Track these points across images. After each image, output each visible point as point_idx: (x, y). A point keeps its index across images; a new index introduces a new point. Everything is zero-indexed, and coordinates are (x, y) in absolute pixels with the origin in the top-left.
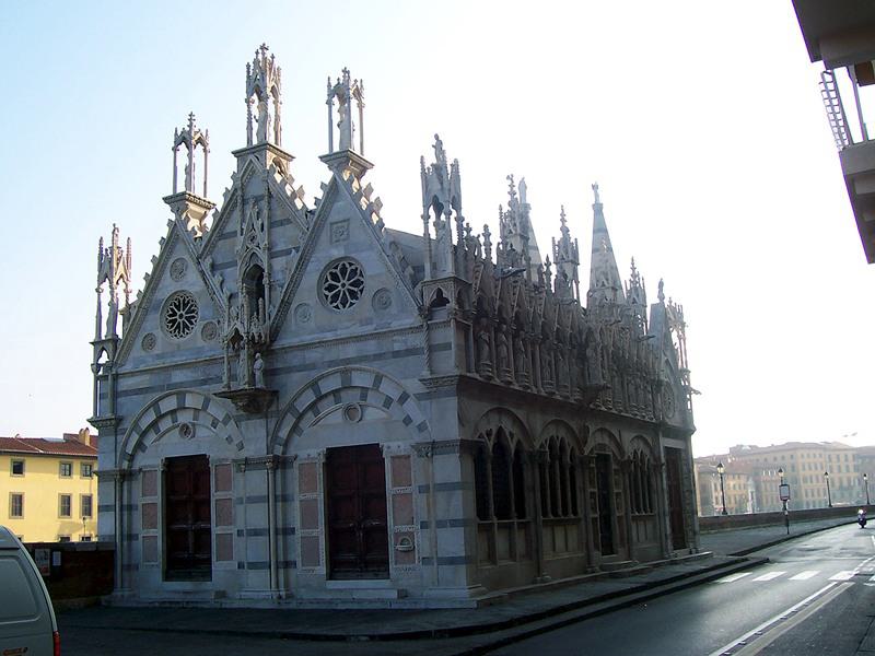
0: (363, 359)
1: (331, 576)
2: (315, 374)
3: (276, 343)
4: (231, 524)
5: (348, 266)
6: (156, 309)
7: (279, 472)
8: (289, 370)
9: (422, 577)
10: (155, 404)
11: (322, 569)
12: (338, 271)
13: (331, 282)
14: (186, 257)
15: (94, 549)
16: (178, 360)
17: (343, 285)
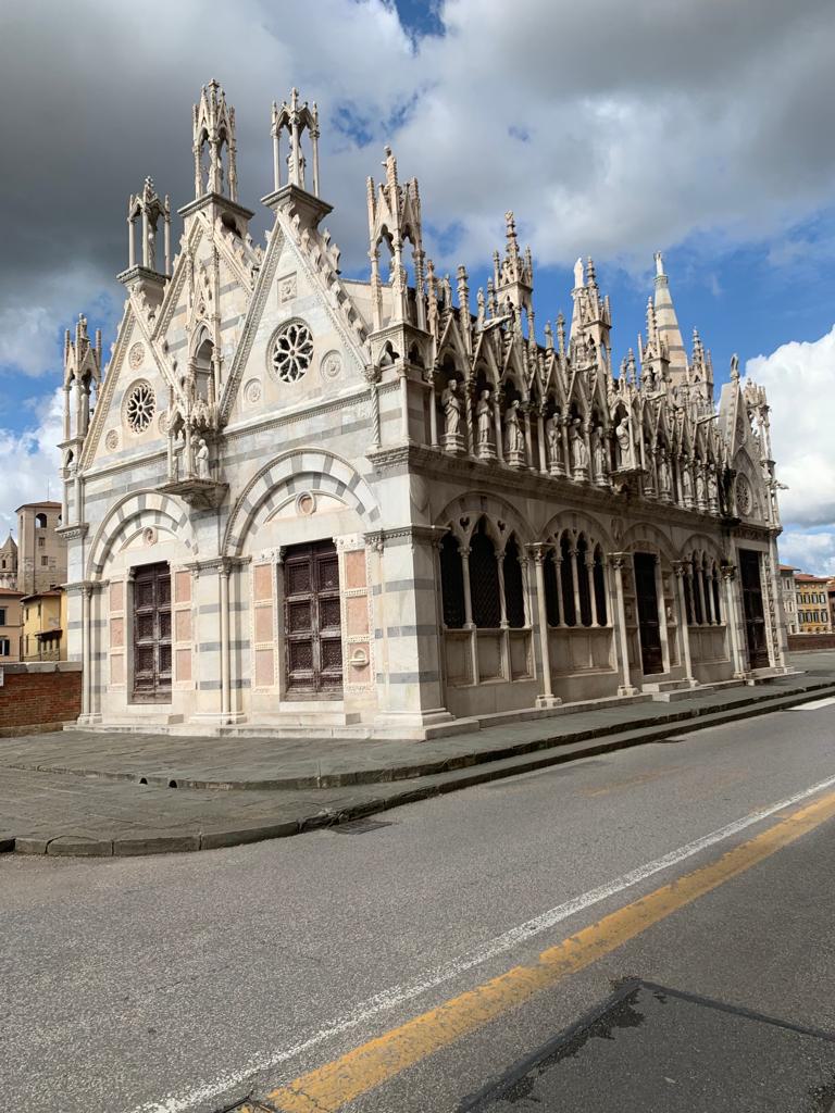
1: (284, 698)
3: (226, 429)
4: (189, 638)
5: (297, 329)
6: (117, 403)
7: (232, 576)
8: (240, 458)
9: (376, 698)
11: (276, 688)
12: (287, 337)
13: (281, 351)
14: (143, 341)
15: (53, 670)
16: (137, 457)
17: (293, 353)
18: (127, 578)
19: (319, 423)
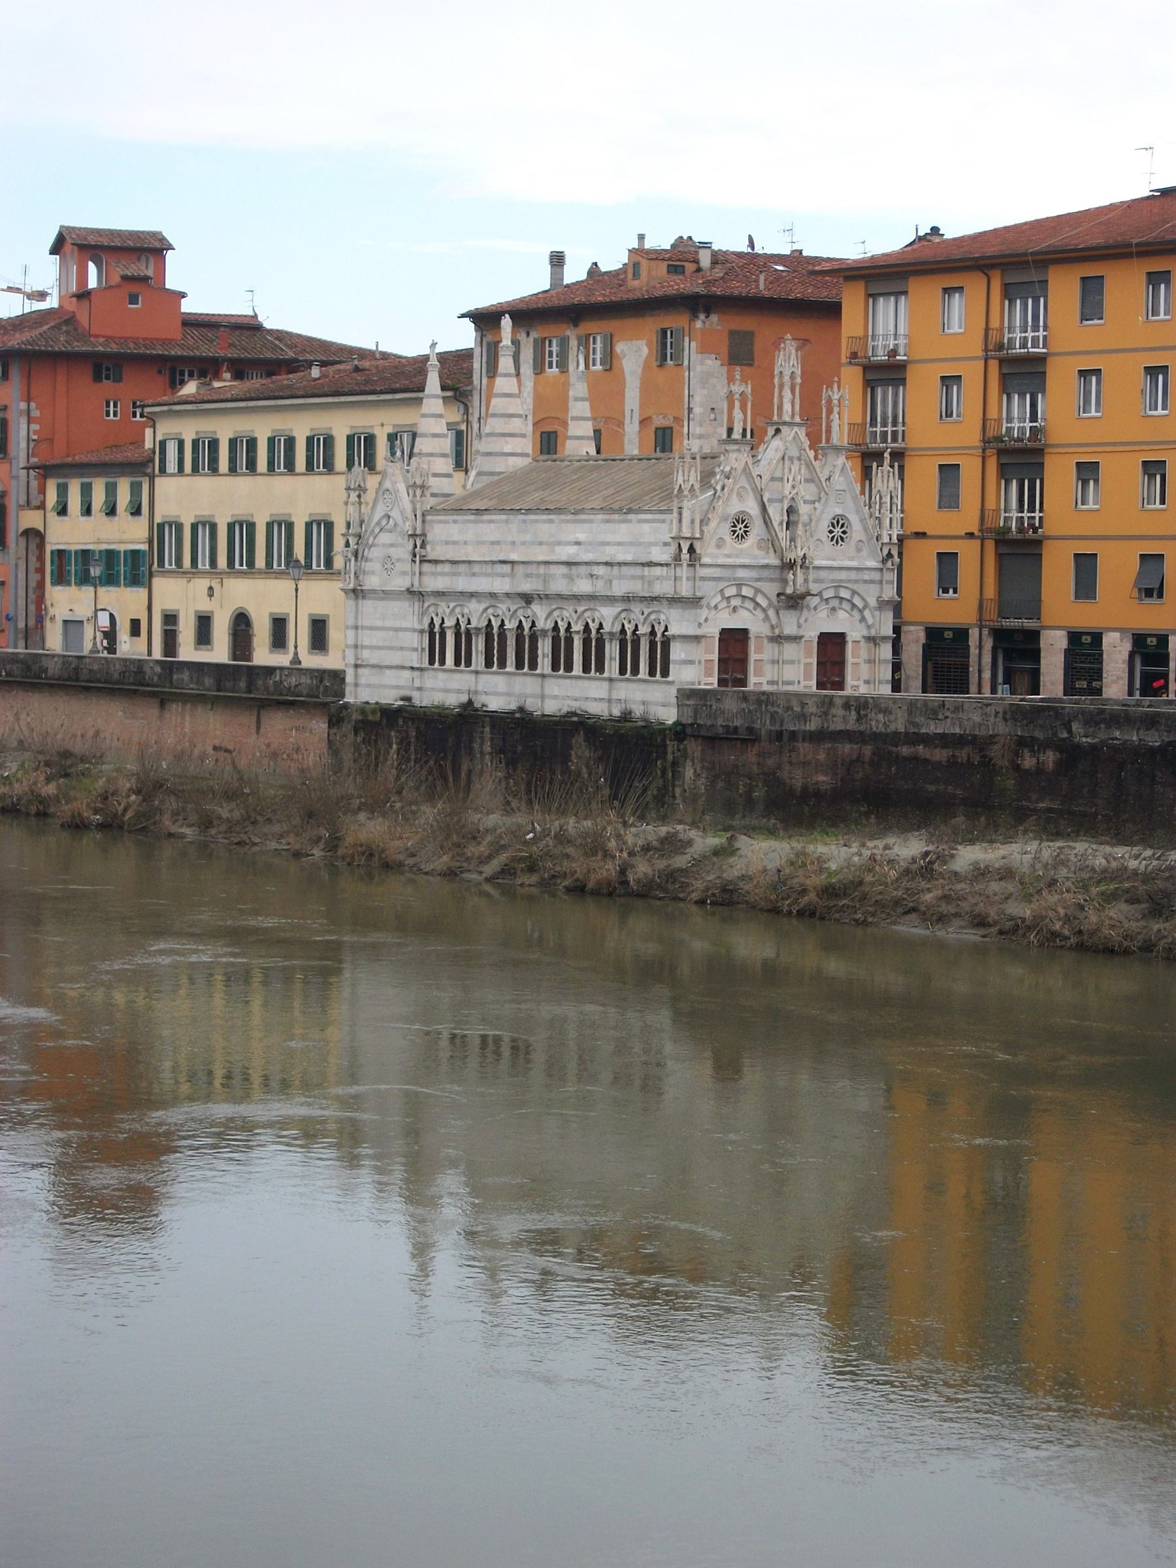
0: (849, 581)
2: (824, 586)
10: (722, 591)
18: (717, 636)
19: (853, 575)
